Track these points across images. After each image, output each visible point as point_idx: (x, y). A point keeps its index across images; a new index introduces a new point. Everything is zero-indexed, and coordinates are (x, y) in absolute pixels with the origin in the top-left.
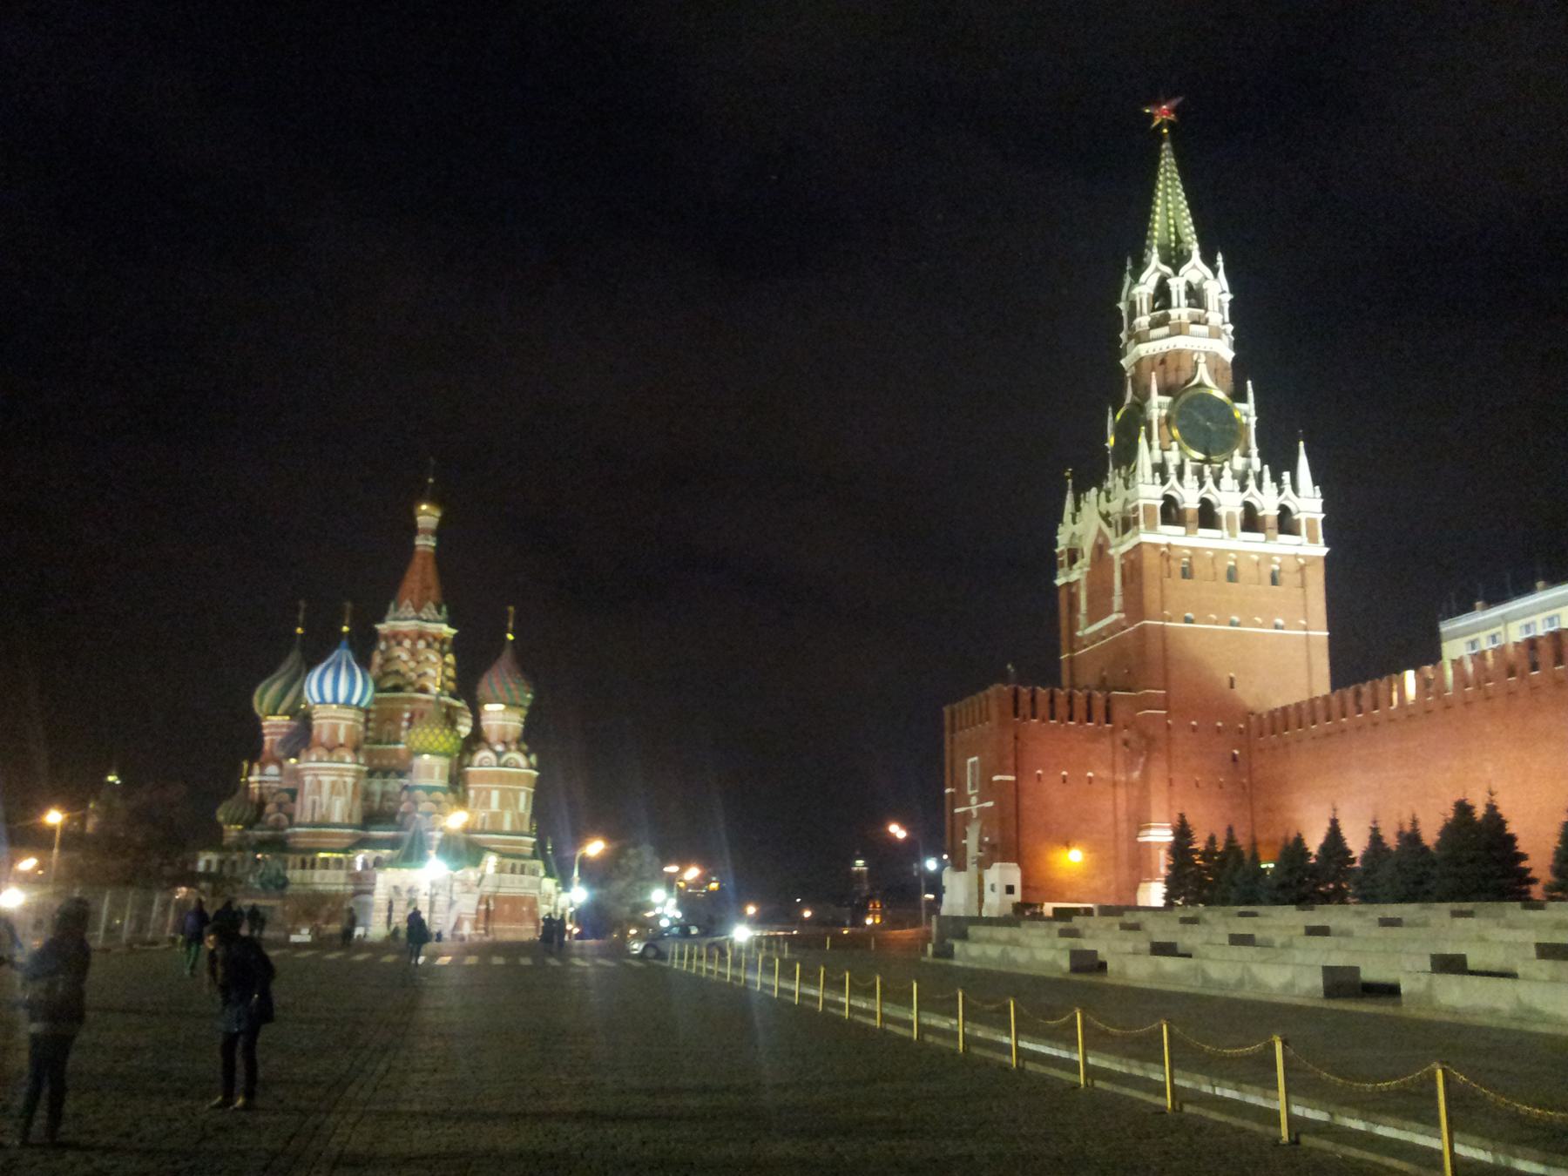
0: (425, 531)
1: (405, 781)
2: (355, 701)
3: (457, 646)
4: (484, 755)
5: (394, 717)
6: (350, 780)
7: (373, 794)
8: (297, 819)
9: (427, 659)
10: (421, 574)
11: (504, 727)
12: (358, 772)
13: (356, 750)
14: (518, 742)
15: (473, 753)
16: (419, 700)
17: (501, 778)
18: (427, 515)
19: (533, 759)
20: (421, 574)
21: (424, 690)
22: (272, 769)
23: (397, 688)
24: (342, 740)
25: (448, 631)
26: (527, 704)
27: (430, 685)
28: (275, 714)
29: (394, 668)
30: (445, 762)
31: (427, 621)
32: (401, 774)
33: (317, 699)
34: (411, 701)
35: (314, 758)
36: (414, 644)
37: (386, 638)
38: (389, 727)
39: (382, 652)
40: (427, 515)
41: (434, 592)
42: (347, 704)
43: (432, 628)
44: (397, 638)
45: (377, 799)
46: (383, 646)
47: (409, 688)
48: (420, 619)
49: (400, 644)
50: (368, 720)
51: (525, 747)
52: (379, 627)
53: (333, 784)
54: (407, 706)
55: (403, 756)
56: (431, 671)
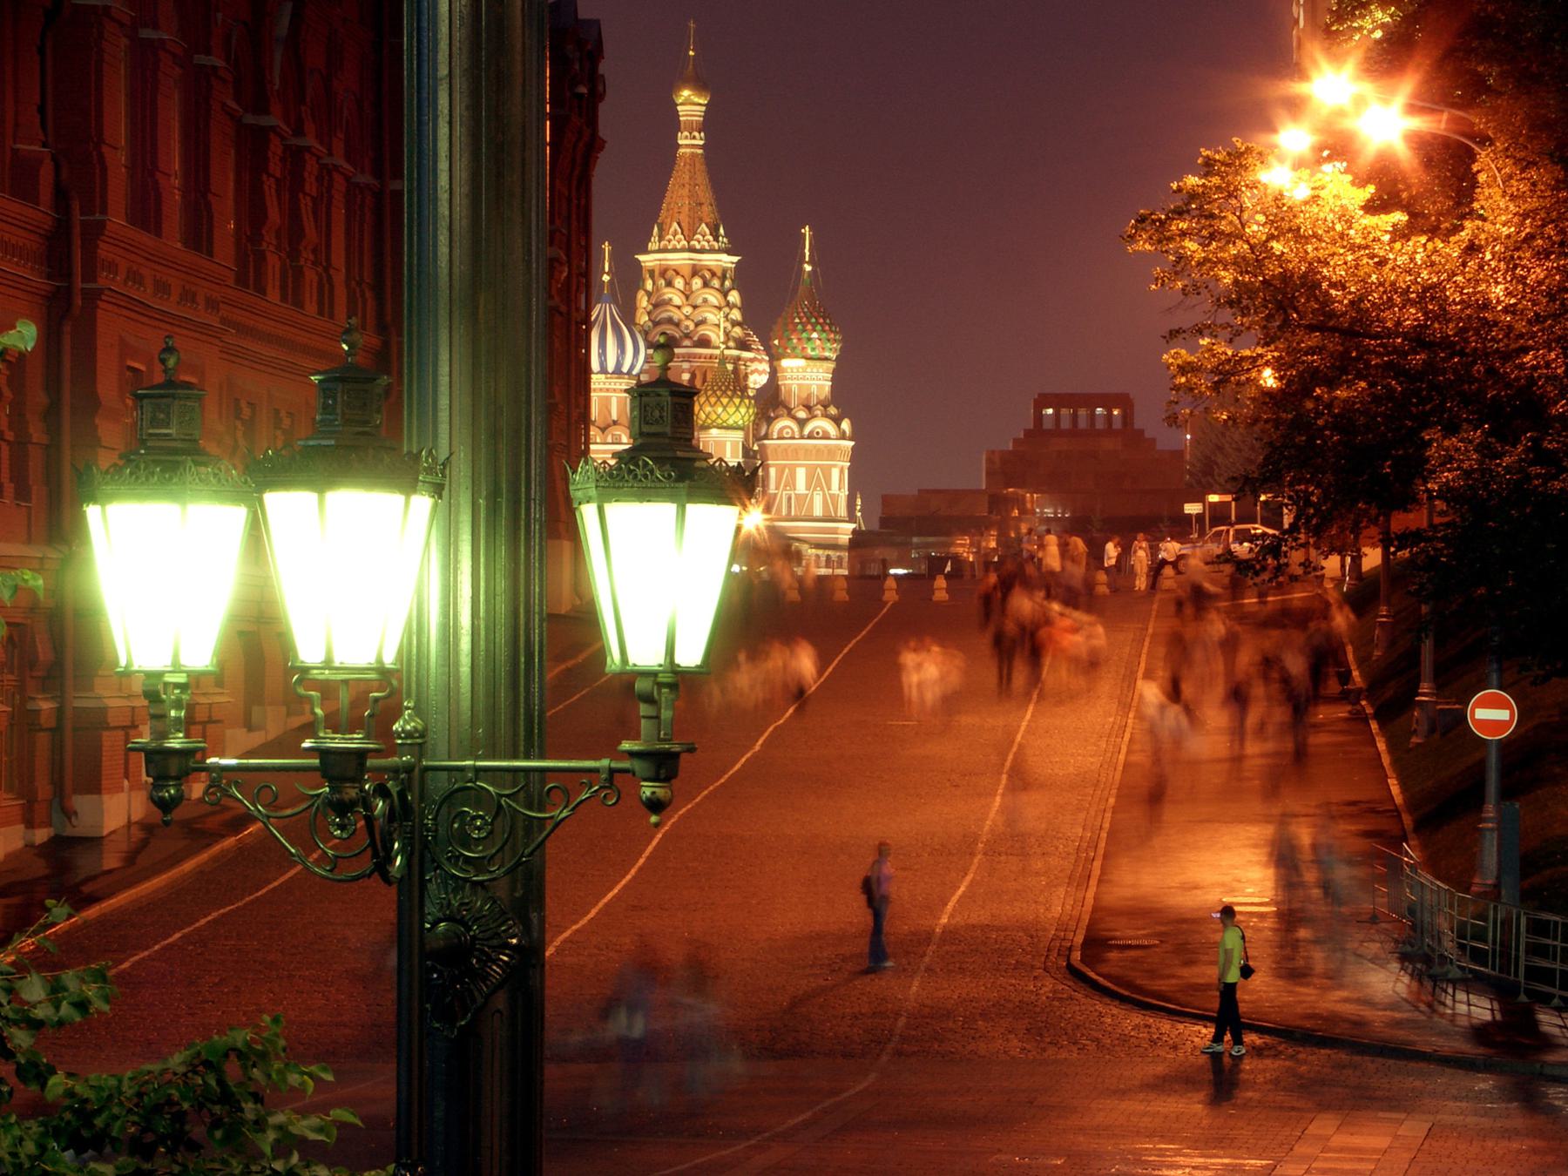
2: (625, 369)
3: (742, 278)
9: (705, 301)
10: (686, 189)
15: (770, 421)
18: (690, 104)
20: (686, 189)
24: (615, 417)
25: (729, 261)
29: (665, 315)
31: (702, 251)
36: (687, 283)
37: (652, 273)
39: (649, 294)
40: (690, 104)
41: (706, 209)
42: (618, 371)
43: (709, 260)
44: (666, 275)
46: (649, 285)
47: (687, 342)
48: (692, 250)
49: (669, 284)
52: (641, 258)
54: (686, 365)
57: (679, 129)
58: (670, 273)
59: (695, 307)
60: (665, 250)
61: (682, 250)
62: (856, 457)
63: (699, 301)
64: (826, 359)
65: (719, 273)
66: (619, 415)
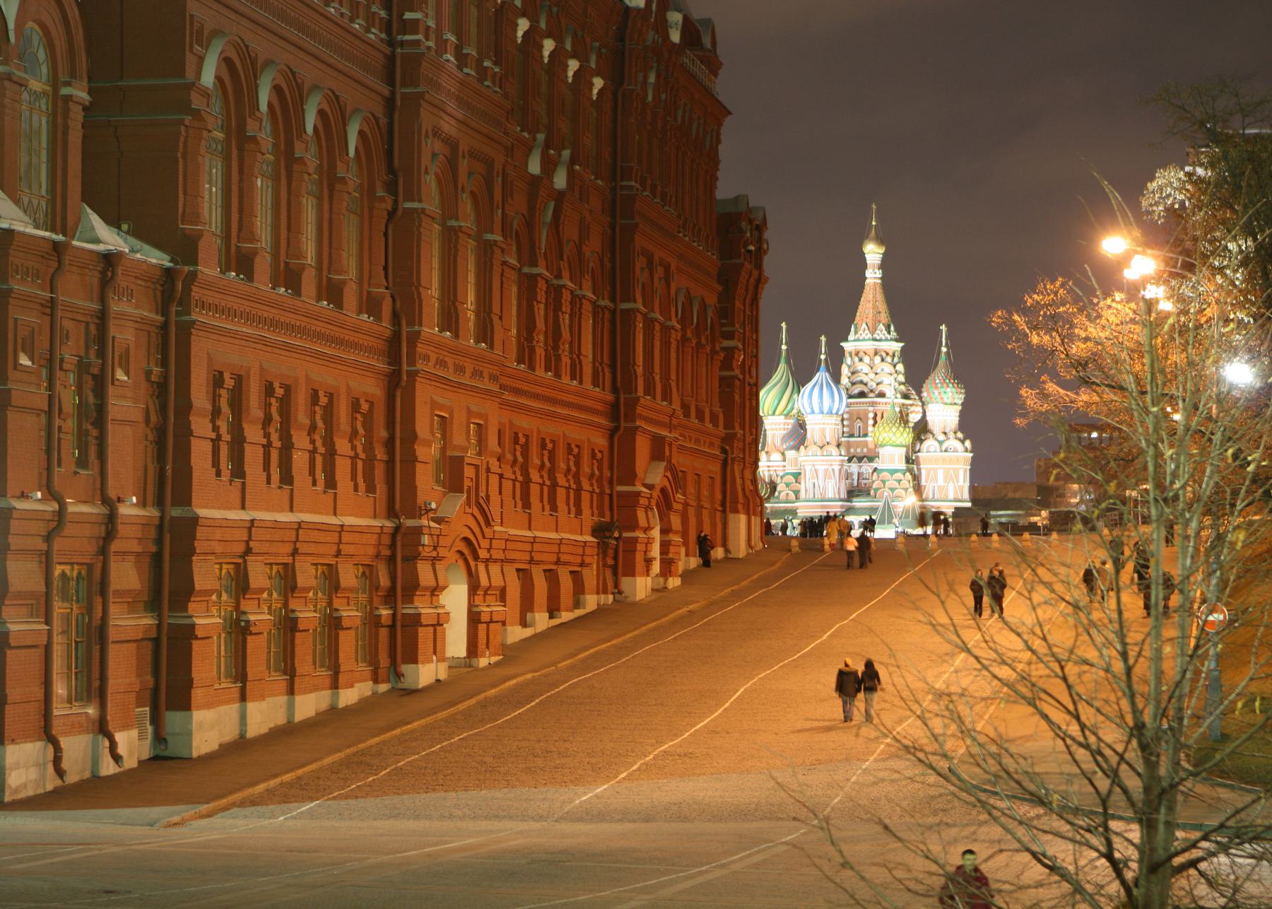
1: (874, 465)
3: (905, 355)
4: (929, 444)
5: (862, 417)
6: (837, 468)
7: (852, 474)
8: (802, 495)
15: (922, 441)
18: (873, 253)
19: (968, 443)
21: (882, 395)
23: (862, 395)
25: (897, 346)
26: (960, 402)
28: (774, 414)
31: (880, 340)
32: (871, 460)
33: (809, 411)
34: (873, 404)
38: (859, 424)
40: (873, 253)
41: (884, 317)
42: (830, 413)
45: (855, 477)
46: (849, 361)
50: (843, 420)
51: (960, 435)
53: (826, 471)
54: (871, 409)
60: (858, 340)
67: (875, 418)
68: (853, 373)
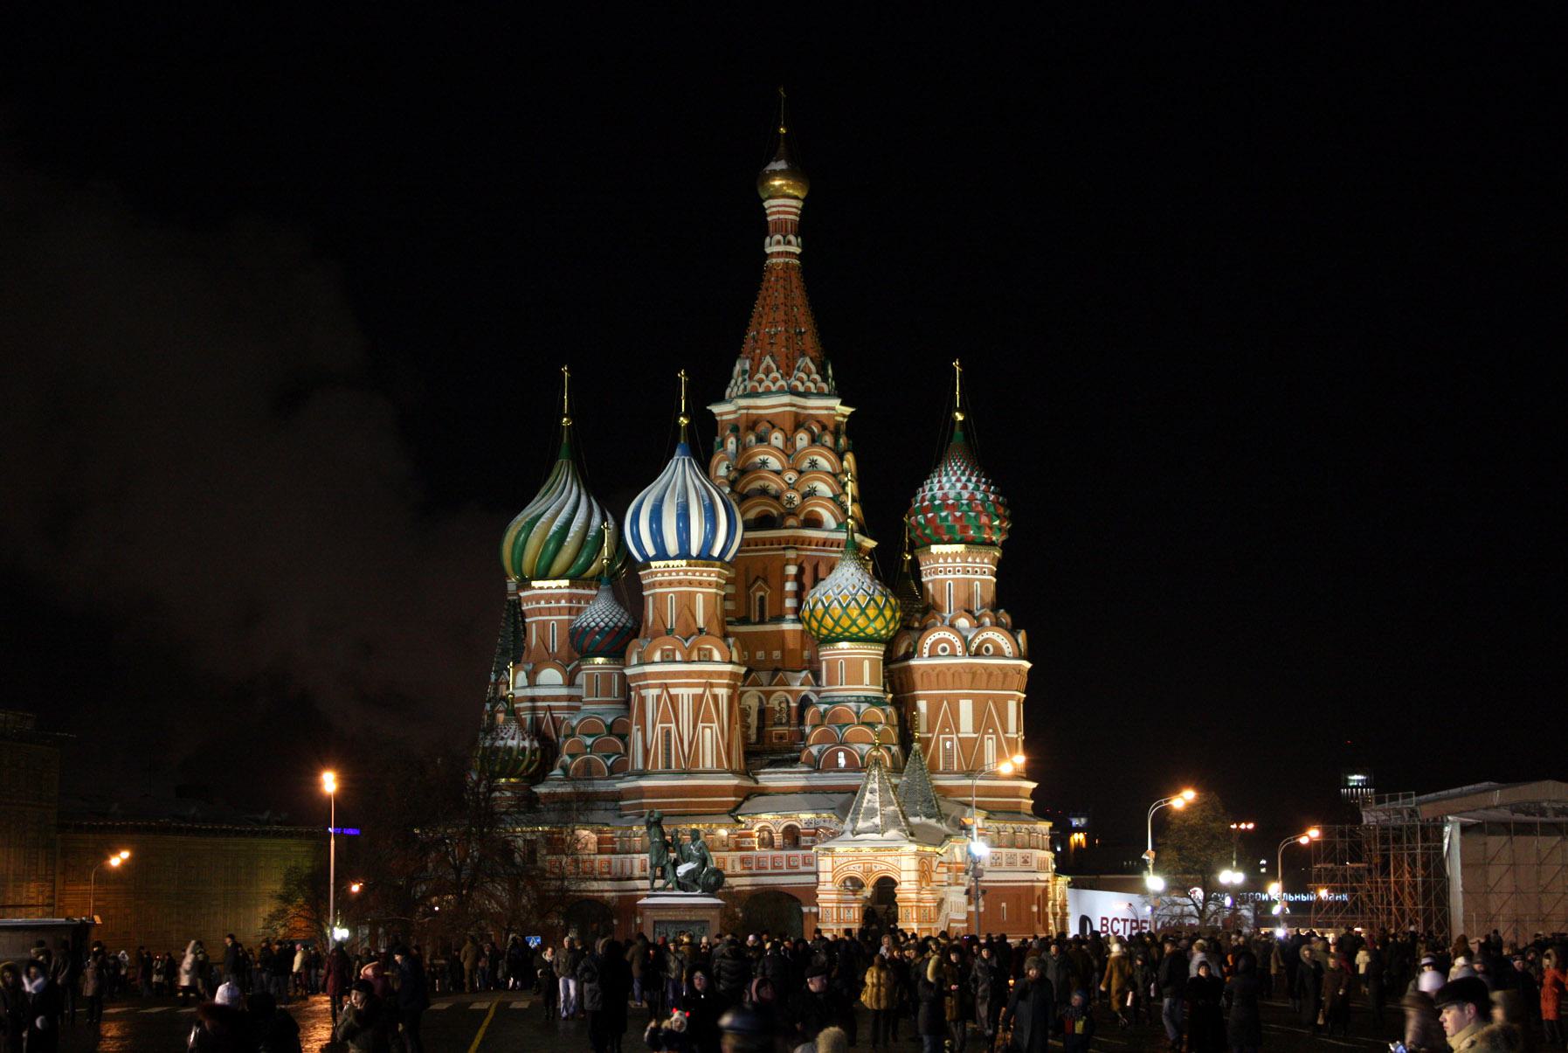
0: (782, 227)
3: (856, 437)
6: (723, 693)
9: (814, 464)
10: (780, 309)
11: (970, 582)
12: (733, 675)
13: (725, 636)
14: (995, 608)
16: (809, 541)
17: (974, 677)
18: (783, 198)
20: (780, 309)
22: (551, 676)
23: (765, 522)
25: (840, 410)
27: (828, 519)
28: (544, 577)
29: (757, 485)
30: (877, 651)
31: (806, 394)
33: (651, 551)
35: (657, 657)
37: (735, 429)
40: (783, 198)
41: (810, 341)
42: (705, 557)
44: (753, 427)
45: (753, 720)
46: (731, 444)
47: (791, 521)
48: (794, 392)
49: (762, 439)
51: (1006, 619)
53: (698, 700)
54: (791, 554)
55: (792, 643)
56: (824, 489)
57: (766, 233)
58: (763, 427)
59: (800, 472)
60: (754, 394)
61: (781, 391)
62: (1035, 686)
63: (806, 465)
64: (992, 544)
65: (831, 427)
66: (707, 622)
67: (798, 578)
68: (743, 472)
